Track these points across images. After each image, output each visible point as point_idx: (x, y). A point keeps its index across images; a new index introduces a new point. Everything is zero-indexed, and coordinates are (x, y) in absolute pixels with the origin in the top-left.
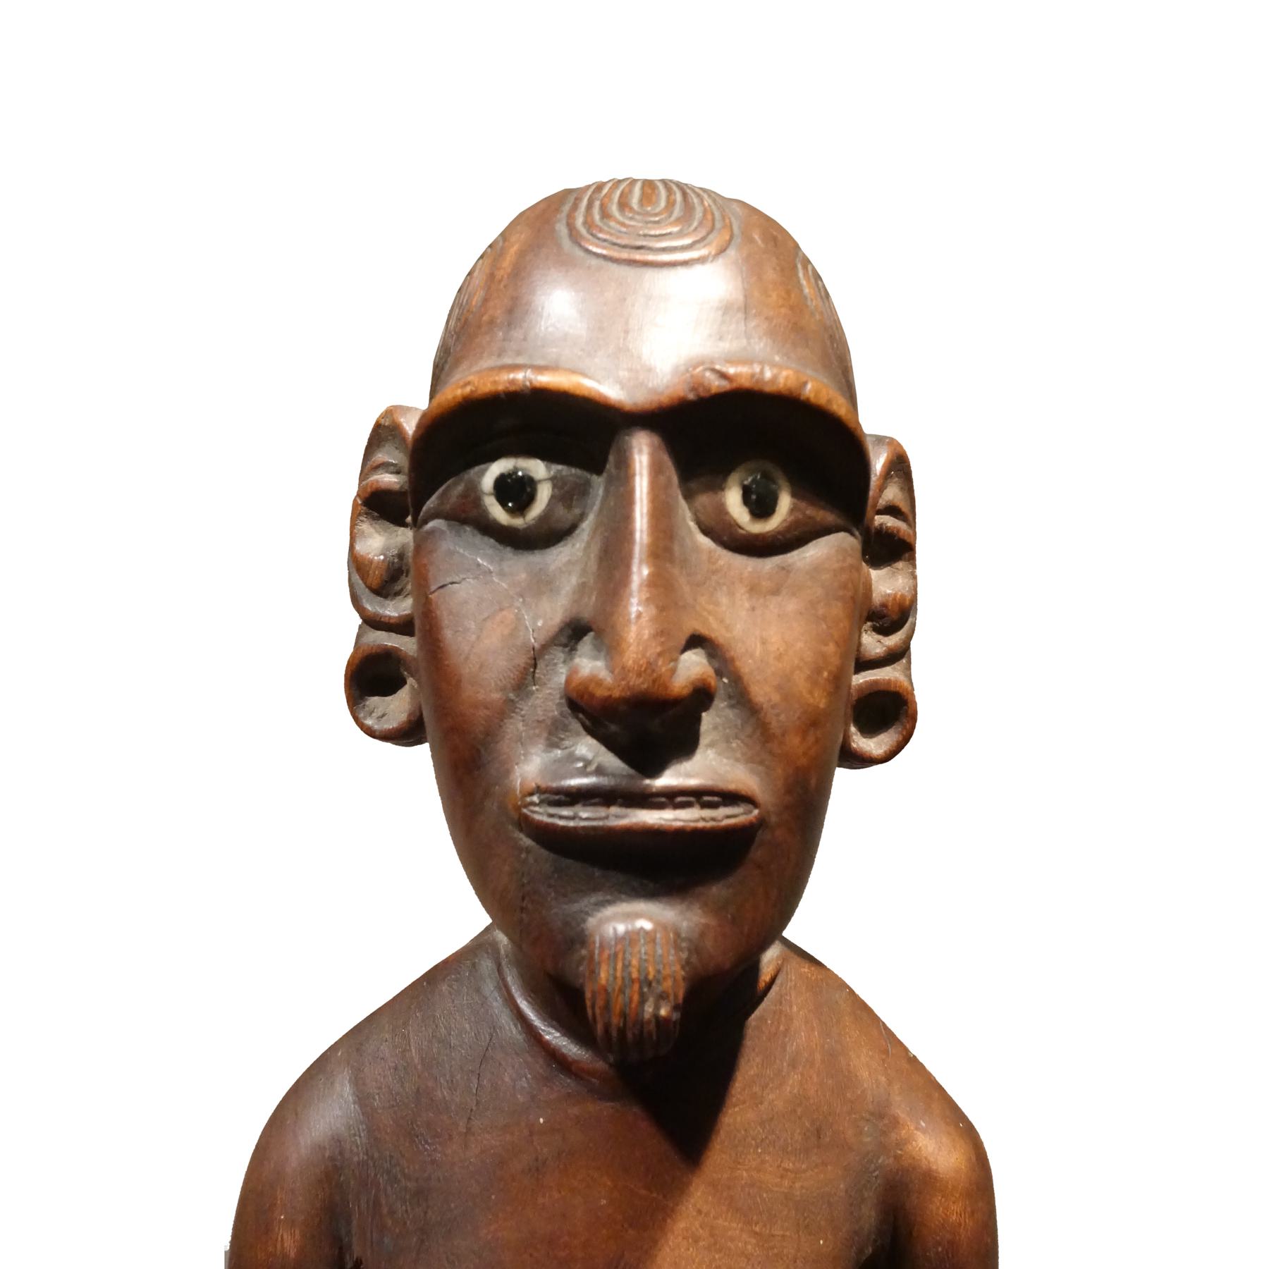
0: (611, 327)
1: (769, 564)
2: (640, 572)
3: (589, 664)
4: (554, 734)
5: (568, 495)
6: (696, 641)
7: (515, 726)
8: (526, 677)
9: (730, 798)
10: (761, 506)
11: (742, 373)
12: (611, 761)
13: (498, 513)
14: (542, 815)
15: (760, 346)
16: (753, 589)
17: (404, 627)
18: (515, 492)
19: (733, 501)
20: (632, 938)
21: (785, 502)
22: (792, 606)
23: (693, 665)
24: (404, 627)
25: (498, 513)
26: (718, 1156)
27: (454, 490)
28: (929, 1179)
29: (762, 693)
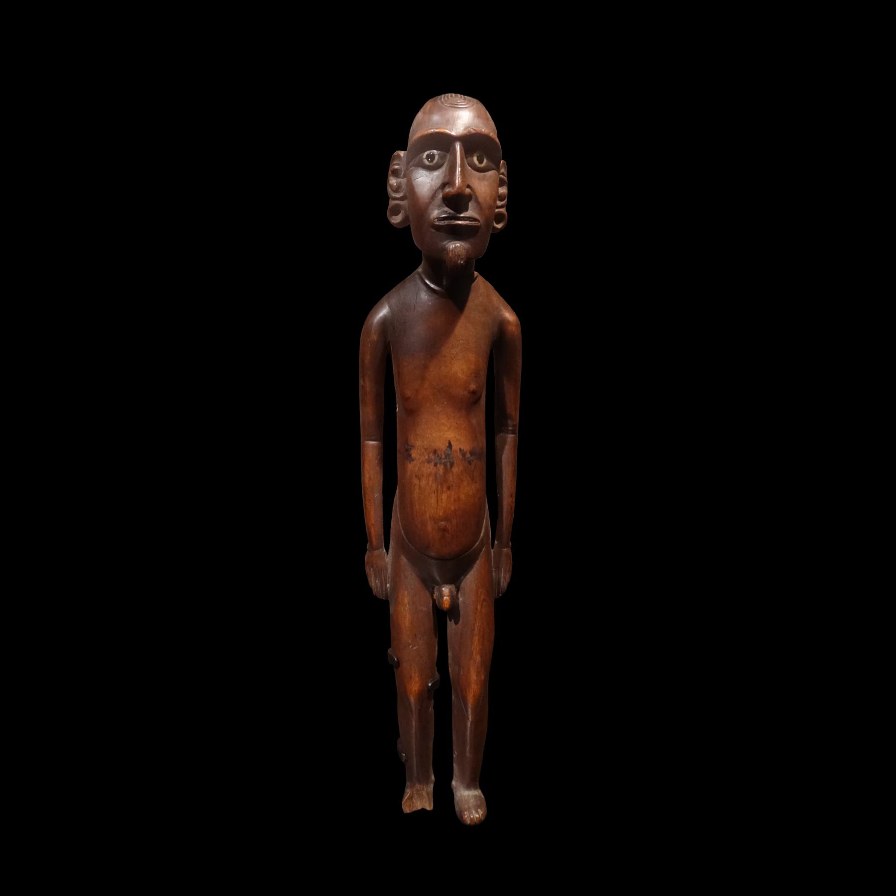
0: (449, 122)
1: (482, 174)
2: (458, 170)
3: (447, 190)
4: (439, 207)
5: (442, 158)
6: (468, 186)
7: (431, 207)
8: (433, 197)
9: (475, 220)
10: (481, 162)
11: (478, 130)
12: (452, 211)
13: (427, 162)
14: (437, 223)
15: (481, 125)
16: (479, 179)
17: (402, 199)
18: (431, 157)
19: (475, 159)
20: (456, 247)
21: (485, 161)
22: (486, 183)
23: (468, 190)
24: (402, 199)
25: (427, 162)
26: (466, 311)
27: (417, 160)
28: (508, 322)
29: (480, 200)
